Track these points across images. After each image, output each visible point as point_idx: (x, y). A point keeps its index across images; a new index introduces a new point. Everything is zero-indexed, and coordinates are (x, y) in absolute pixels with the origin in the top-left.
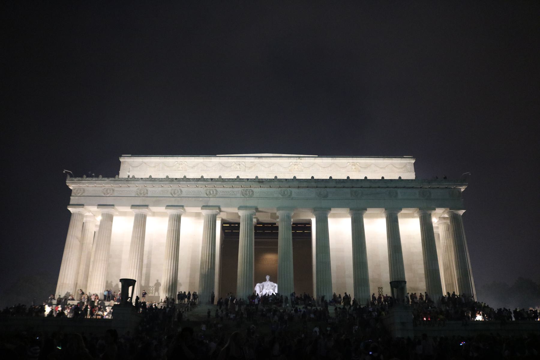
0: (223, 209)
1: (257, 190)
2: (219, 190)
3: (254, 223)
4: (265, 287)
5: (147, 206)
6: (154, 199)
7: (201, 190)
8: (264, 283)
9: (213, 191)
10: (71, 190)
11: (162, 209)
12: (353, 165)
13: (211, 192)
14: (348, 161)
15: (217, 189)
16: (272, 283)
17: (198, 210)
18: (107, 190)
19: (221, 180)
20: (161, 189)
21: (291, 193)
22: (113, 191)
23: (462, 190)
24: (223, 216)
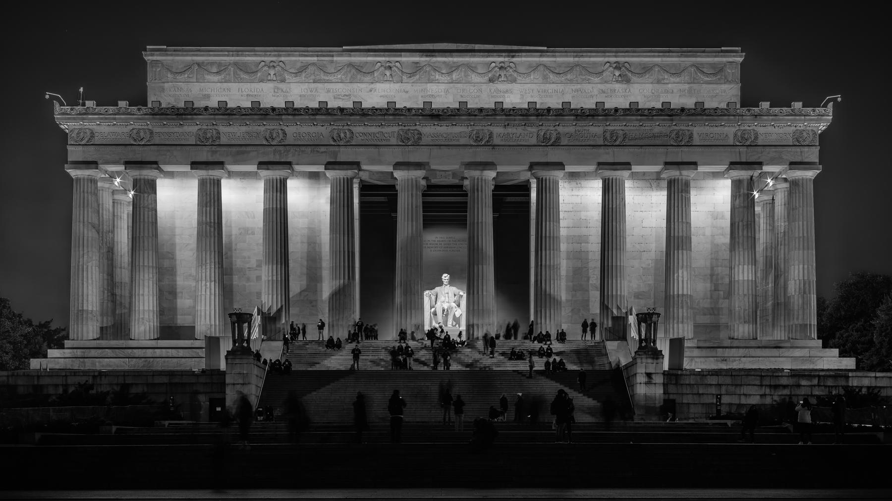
0: (364, 167)
1: (429, 130)
3: (422, 188)
4: (441, 298)
6: (234, 149)
7: (321, 130)
8: (437, 289)
12: (616, 68)
13: (342, 135)
14: (607, 59)
15: (351, 128)
17: (320, 168)
18: (138, 133)
20: (244, 129)
21: (491, 135)
22: (152, 133)
23: (823, 127)
24: (365, 176)
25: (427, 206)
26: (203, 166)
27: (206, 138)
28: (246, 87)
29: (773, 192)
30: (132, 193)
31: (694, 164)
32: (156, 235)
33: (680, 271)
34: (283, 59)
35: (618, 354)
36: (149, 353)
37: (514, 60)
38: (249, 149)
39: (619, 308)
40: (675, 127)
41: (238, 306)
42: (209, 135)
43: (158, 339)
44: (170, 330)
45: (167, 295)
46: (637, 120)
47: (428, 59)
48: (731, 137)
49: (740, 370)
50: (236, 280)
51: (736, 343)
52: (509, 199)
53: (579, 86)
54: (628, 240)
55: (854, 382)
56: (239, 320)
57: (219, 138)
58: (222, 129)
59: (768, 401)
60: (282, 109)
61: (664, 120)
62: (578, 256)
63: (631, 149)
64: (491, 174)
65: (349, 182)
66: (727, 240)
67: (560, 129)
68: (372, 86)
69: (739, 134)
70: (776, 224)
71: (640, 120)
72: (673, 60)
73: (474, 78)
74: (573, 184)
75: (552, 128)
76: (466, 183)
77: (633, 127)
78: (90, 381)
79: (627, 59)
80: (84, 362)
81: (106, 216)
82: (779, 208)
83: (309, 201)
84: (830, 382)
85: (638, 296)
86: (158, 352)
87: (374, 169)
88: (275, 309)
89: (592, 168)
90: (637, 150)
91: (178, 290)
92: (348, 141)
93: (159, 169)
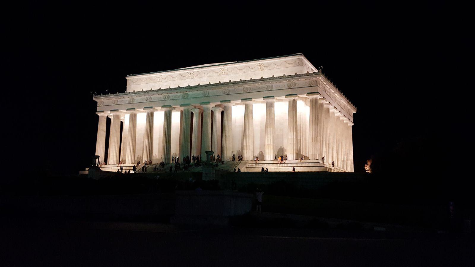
2: (171, 95)
5: (134, 109)
7: (161, 96)
9: (167, 96)
10: (97, 102)
11: (142, 110)
13: (166, 97)
15: (169, 94)
19: (170, 89)
21: (209, 92)
22: (117, 101)
27: (131, 101)
34: (161, 75)
37: (227, 67)
42: (132, 101)
58: (135, 98)
63: (252, 93)
69: (289, 85)
73: (215, 74)
77: (252, 85)
79: (263, 62)
92: (168, 99)
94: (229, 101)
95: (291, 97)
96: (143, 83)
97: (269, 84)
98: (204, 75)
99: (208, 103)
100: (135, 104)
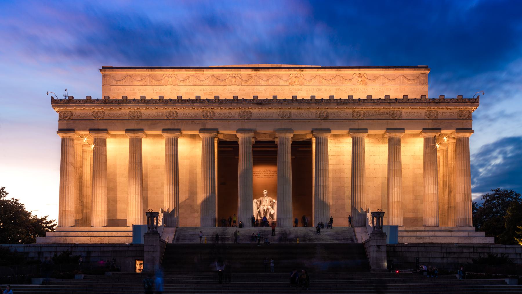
0: (221, 131)
1: (256, 111)
6: (149, 122)
7: (197, 111)
8: (261, 198)
9: (210, 113)
13: (208, 114)
14: (354, 72)
15: (213, 110)
16: (270, 198)
17: (196, 132)
18: (97, 113)
20: (155, 111)
21: (290, 113)
22: (104, 113)
24: (221, 137)
25: (255, 153)
26: (132, 131)
27: (134, 117)
28: (156, 88)
29: (447, 145)
30: (93, 146)
31: (402, 130)
32: (106, 169)
33: (396, 189)
35: (361, 236)
36: (102, 234)
37: (303, 73)
38: (157, 122)
39: (361, 209)
40: (392, 109)
41: (152, 208)
43: (106, 226)
44: (113, 221)
45: (112, 203)
46: (371, 105)
47: (255, 72)
48: (423, 114)
49: (430, 243)
50: (150, 194)
51: (427, 229)
52: (300, 149)
53: (338, 87)
54: (367, 171)
55: (494, 251)
56: (151, 215)
57: (141, 116)
59: (445, 261)
60: (176, 100)
61: (386, 105)
62: (339, 180)
64: (290, 136)
65: (212, 140)
66: (422, 171)
67: (329, 111)
68: (225, 87)
70: (449, 162)
71: (373, 106)
72: (391, 72)
73: (281, 82)
74: (336, 140)
75: (324, 110)
76: (277, 140)
77: (369, 108)
78: (69, 250)
80: (66, 239)
81: (79, 158)
82: (451, 153)
83: (191, 150)
84: (480, 251)
85: (372, 202)
86: (107, 234)
87: (226, 133)
88: (170, 210)
89: (346, 132)
90: (371, 121)
91: (118, 199)
93: (108, 133)
94: (329, 130)
95: (431, 132)
96: (140, 83)
97: (396, 108)
98: (261, 82)
99: (290, 130)
100: (143, 122)
